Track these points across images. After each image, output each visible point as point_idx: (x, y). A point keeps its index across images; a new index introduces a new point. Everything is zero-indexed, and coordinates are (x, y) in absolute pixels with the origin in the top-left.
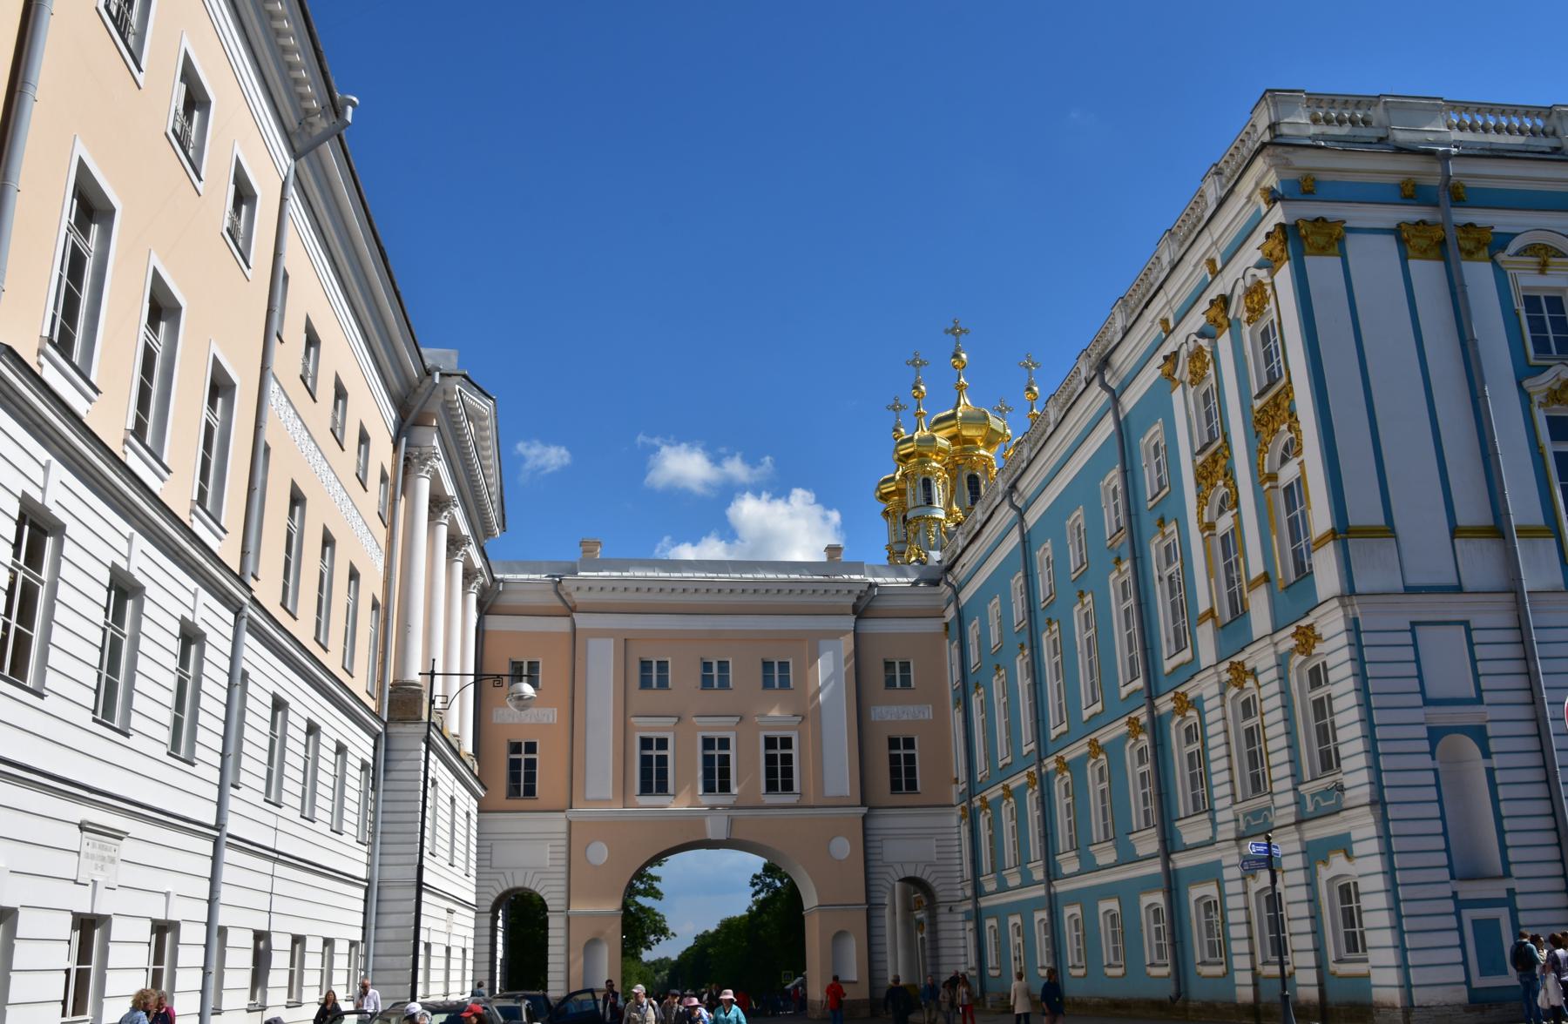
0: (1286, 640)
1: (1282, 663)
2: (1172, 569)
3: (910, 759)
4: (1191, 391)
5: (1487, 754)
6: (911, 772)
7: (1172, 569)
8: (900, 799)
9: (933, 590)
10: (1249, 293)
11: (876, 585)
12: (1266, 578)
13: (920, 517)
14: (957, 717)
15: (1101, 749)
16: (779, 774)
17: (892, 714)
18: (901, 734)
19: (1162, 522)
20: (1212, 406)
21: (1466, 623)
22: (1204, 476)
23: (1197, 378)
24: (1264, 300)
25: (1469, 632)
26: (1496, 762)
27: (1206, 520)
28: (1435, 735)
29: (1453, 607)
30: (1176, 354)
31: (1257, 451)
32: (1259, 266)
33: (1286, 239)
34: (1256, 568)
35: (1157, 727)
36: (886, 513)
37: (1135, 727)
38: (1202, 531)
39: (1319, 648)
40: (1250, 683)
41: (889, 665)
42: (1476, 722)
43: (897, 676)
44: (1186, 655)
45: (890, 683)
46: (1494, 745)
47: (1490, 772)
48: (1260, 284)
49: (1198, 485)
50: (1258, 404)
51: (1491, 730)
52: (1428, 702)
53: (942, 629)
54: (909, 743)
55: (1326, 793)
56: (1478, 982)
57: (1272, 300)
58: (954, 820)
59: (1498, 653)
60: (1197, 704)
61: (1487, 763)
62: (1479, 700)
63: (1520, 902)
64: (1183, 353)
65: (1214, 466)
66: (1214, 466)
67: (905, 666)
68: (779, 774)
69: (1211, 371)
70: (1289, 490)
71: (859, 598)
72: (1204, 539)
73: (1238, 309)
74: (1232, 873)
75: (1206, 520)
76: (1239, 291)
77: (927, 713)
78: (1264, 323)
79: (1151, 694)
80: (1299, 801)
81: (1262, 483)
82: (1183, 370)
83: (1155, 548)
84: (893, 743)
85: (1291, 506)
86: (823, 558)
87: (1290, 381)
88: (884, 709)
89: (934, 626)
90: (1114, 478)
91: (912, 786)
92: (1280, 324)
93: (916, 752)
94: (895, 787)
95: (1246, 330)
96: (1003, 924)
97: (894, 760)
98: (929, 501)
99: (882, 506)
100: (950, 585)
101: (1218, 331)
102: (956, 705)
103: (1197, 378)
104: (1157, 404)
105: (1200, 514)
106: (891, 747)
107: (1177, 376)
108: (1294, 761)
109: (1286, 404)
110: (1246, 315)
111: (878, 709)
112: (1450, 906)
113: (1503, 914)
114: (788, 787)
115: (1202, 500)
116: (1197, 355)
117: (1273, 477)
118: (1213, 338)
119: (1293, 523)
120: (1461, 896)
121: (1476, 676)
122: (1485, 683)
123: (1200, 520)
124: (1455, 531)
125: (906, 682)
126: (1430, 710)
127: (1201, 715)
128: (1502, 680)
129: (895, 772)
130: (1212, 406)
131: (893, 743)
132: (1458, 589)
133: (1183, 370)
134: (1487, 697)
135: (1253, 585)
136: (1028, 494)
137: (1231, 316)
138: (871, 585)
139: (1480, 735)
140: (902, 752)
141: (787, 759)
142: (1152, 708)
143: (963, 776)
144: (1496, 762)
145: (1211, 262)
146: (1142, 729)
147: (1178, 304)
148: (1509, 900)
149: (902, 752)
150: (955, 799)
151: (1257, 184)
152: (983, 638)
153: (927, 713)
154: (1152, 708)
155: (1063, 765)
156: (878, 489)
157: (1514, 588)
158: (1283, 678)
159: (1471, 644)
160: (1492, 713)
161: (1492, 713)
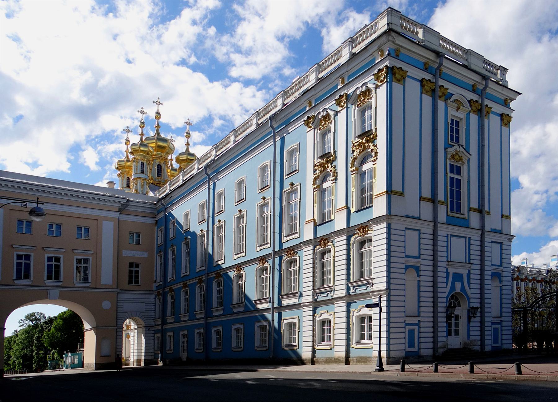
3: (137, 272)
5: (419, 276)
8: (131, 287)
17: (132, 254)
21: (419, 230)
25: (420, 233)
26: (422, 278)
28: (407, 267)
42: (418, 265)
46: (422, 273)
47: (419, 281)
51: (422, 268)
52: (406, 256)
53: (154, 222)
54: (137, 266)
56: (408, 350)
59: (427, 242)
61: (418, 279)
62: (419, 257)
63: (422, 324)
67: (138, 235)
77: (145, 255)
84: (131, 265)
88: (128, 252)
89: (151, 221)
93: (140, 269)
94: (130, 282)
97: (131, 272)
106: (129, 267)
111: (126, 251)
112: (403, 325)
113: (416, 328)
120: (406, 322)
121: (420, 249)
122: (423, 252)
126: (406, 259)
128: (427, 252)
129: (130, 277)
131: (131, 265)
132: (419, 219)
134: (422, 257)
139: (417, 269)
140: (134, 269)
144: (422, 278)
148: (418, 324)
149: (134, 269)
157: (435, 221)
159: (420, 238)
160: (423, 262)
161: (423, 262)
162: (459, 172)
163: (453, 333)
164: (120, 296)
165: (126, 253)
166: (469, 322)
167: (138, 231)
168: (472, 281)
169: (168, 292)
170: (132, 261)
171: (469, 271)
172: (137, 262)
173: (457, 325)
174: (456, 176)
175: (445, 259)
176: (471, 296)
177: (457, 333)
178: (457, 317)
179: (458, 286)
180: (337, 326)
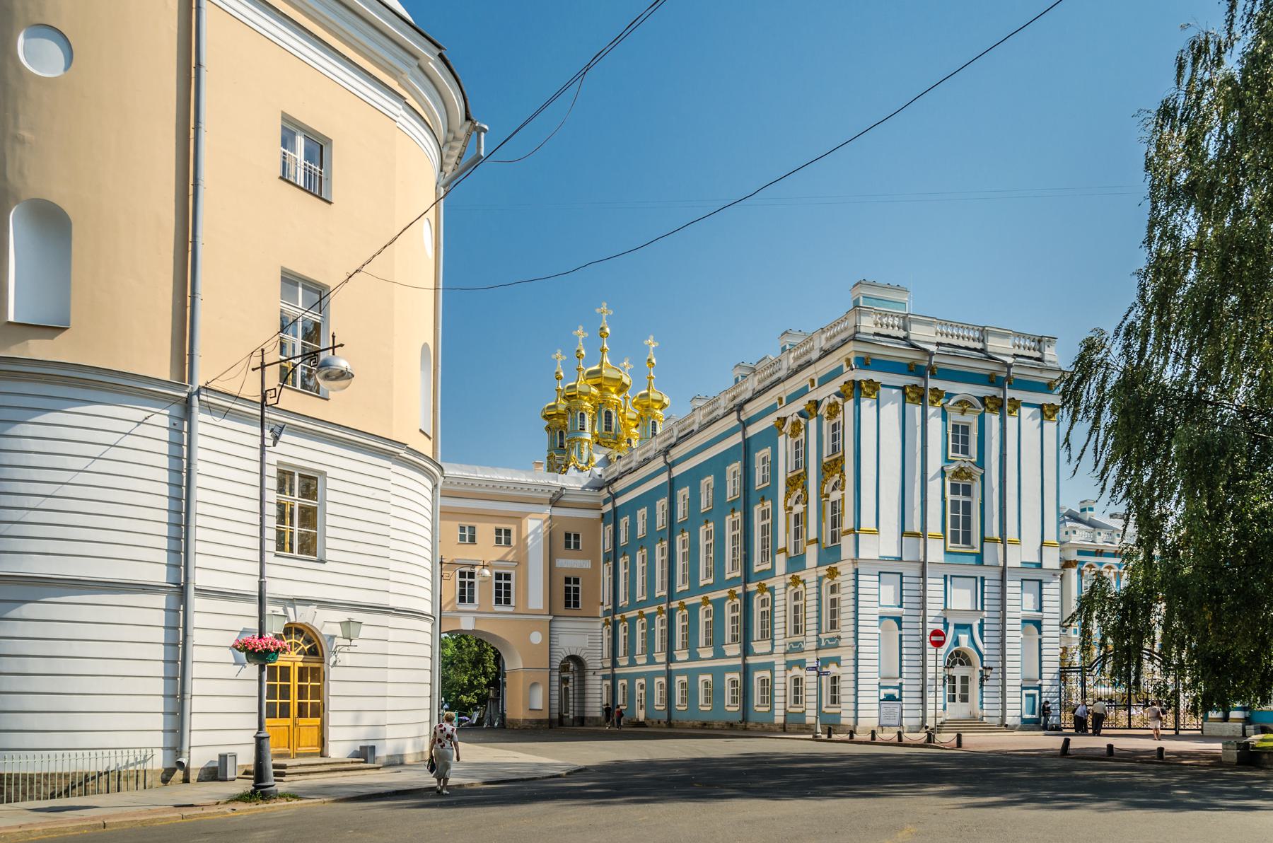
0: (823, 571)
1: (820, 580)
2: (765, 522)
3: (577, 590)
4: (790, 439)
5: (900, 628)
6: (576, 597)
7: (765, 522)
8: (568, 612)
9: (596, 493)
12: (817, 541)
14: (606, 571)
15: (710, 602)
16: (503, 594)
17: (568, 563)
18: (572, 575)
19: (763, 499)
20: (800, 451)
23: (794, 433)
26: (904, 632)
29: (897, 567)
30: (785, 419)
31: (821, 483)
34: (813, 535)
35: (747, 598)
37: (733, 595)
39: (838, 578)
40: (801, 586)
41: (568, 536)
43: (571, 541)
44: (768, 566)
45: (568, 545)
46: (904, 625)
47: (901, 636)
50: (825, 460)
54: (576, 581)
55: (832, 639)
58: (600, 626)
60: (772, 590)
62: (901, 606)
64: (789, 421)
65: (797, 481)
66: (797, 481)
67: (577, 536)
68: (503, 594)
70: (834, 503)
73: (823, 410)
74: (779, 668)
76: (826, 403)
77: (587, 564)
79: (747, 578)
80: (819, 641)
82: (787, 428)
84: (568, 580)
85: (834, 511)
90: (737, 467)
91: (576, 605)
94: (568, 605)
95: (825, 422)
96: (632, 684)
97: (568, 590)
102: (606, 560)
103: (794, 433)
104: (769, 437)
105: (786, 502)
108: (819, 624)
114: (508, 602)
115: (788, 495)
117: (827, 496)
119: (834, 519)
124: (903, 533)
125: (577, 546)
127: (773, 595)
129: (567, 597)
130: (800, 451)
131: (568, 580)
133: (787, 428)
135: (810, 543)
140: (572, 586)
141: (507, 586)
142: (745, 587)
143: (606, 602)
146: (738, 596)
150: (601, 614)
152: (633, 526)
153: (587, 564)
154: (745, 587)
155: (682, 606)
158: (819, 587)
159: (902, 582)
162: (967, 491)
163: (957, 698)
164: (554, 624)
165: (561, 563)
166: (982, 686)
167: (576, 531)
168: (985, 633)
169: (620, 621)
170: (568, 575)
171: (982, 621)
172: (576, 576)
173: (965, 689)
174: (961, 498)
175: (942, 607)
176: (985, 652)
177: (965, 699)
178: (965, 679)
179: (964, 639)
180: (808, 686)
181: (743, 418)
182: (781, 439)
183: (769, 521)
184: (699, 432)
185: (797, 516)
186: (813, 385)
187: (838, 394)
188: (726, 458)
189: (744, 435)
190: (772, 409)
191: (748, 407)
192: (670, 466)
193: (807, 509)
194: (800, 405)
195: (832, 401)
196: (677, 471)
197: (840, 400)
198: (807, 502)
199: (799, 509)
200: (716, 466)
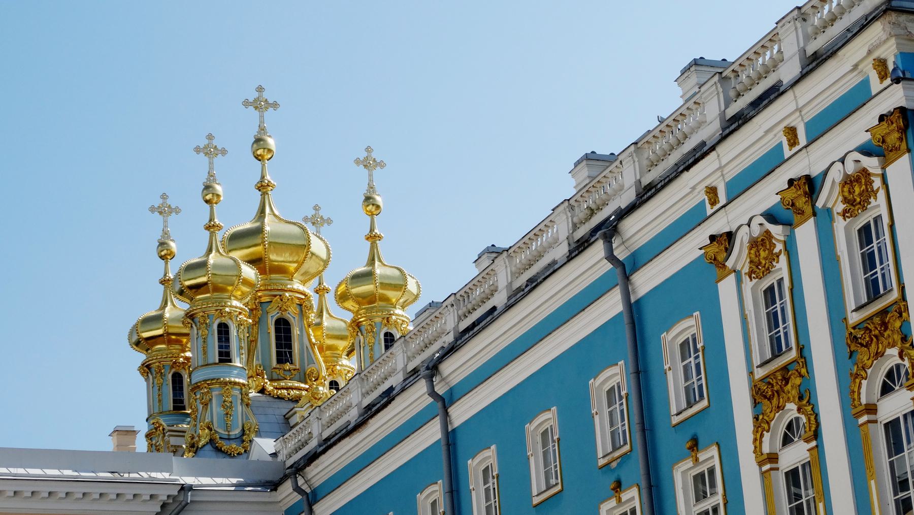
4: (748, 285)
9: (267, 496)
10: (849, 181)
11: (190, 488)
13: (210, 382)
19: (695, 445)
20: (778, 309)
22: (765, 394)
23: (759, 269)
24: (869, 193)
27: (766, 449)
30: (730, 236)
32: (866, 150)
33: (906, 127)
36: (146, 369)
38: (761, 464)
48: (865, 173)
49: (755, 404)
50: (854, 318)
57: (881, 194)
65: (784, 382)
66: (784, 382)
69: (782, 263)
71: (164, 506)
72: (763, 474)
73: (830, 196)
75: (766, 449)
76: (836, 175)
78: (865, 218)
81: (858, 415)
83: (681, 477)
86: (108, 445)
87: (903, 298)
90: (616, 375)
92: (892, 226)
95: (840, 225)
98: (225, 357)
99: (140, 357)
100: (297, 489)
101: (796, 218)
105: (758, 441)
107: (729, 264)
109: (898, 324)
110: (840, 207)
115: (761, 424)
116: (761, 243)
117: (871, 409)
118: (789, 224)
123: (757, 450)
130: (778, 309)
133: (739, 258)
136: (455, 380)
137: (819, 204)
138: (184, 489)
145: (791, 133)
147: (732, 172)
151: (870, 52)
156: (135, 329)
181: (621, 254)
182: (727, 287)
183: (718, 499)
184: (508, 307)
185: (793, 476)
186: (793, 142)
187: (866, 150)
188: (585, 357)
189: (626, 295)
190: (696, 218)
191: (629, 226)
192: (444, 403)
193: (818, 450)
194: (767, 194)
195: (850, 168)
196: (460, 413)
197: (872, 164)
198: (816, 435)
199: (795, 455)
200: (564, 382)
